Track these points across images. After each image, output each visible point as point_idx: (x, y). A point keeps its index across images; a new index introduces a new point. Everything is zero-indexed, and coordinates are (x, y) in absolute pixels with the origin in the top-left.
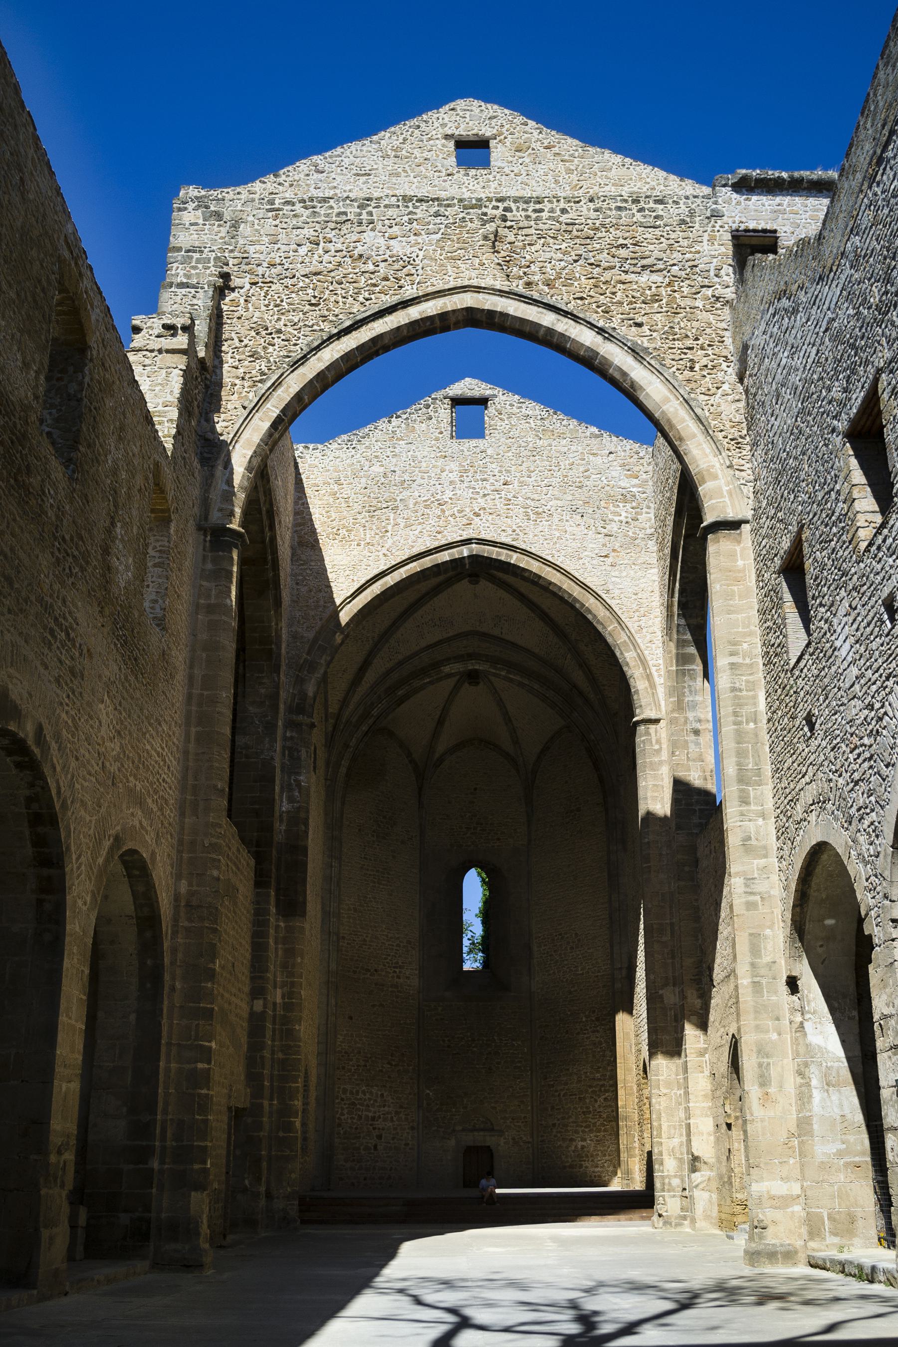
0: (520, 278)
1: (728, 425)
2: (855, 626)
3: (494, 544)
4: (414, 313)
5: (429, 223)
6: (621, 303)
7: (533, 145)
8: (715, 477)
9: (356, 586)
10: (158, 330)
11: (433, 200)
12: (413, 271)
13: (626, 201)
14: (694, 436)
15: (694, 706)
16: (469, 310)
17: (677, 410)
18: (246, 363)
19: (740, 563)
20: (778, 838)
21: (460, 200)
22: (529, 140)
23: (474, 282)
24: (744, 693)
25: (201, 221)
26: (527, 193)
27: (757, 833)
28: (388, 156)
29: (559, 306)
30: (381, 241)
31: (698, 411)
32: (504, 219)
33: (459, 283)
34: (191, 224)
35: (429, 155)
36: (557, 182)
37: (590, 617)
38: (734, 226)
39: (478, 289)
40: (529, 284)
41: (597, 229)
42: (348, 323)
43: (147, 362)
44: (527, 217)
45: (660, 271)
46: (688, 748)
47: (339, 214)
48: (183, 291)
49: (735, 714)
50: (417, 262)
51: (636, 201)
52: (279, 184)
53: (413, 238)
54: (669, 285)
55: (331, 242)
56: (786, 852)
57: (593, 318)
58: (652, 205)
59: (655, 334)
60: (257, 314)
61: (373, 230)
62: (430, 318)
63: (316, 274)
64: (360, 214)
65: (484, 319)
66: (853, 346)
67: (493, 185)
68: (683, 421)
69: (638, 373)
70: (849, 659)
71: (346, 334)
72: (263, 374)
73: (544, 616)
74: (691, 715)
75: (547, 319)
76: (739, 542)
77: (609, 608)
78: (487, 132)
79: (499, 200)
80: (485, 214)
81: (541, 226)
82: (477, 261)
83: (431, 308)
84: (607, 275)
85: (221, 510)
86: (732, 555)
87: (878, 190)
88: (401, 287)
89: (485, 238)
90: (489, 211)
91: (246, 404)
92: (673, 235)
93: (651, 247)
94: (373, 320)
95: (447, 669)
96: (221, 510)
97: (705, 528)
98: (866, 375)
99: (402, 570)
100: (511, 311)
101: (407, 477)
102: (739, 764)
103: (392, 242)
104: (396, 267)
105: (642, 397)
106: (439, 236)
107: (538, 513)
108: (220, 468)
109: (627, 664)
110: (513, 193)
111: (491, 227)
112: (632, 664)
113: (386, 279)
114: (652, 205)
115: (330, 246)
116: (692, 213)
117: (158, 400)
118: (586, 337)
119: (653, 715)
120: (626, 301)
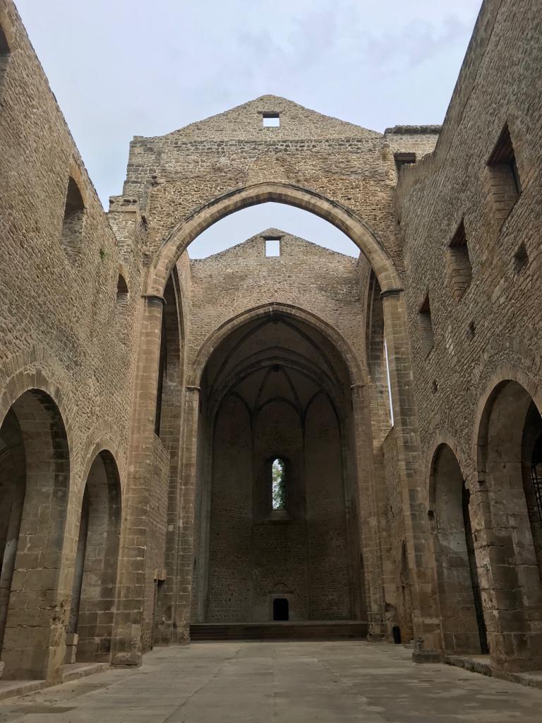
1: (393, 245)
2: (455, 338)
3: (284, 305)
4: (244, 195)
5: (250, 153)
6: (341, 189)
7: (300, 116)
8: (387, 270)
9: (220, 325)
11: (253, 142)
13: (344, 141)
14: (377, 251)
15: (379, 379)
16: (270, 193)
17: (368, 239)
18: (165, 219)
19: (400, 310)
20: (422, 442)
21: (266, 142)
22: (297, 113)
23: (272, 180)
24: (403, 372)
25: (143, 152)
26: (297, 138)
27: (411, 439)
28: (231, 122)
30: (229, 161)
31: (379, 239)
32: (286, 150)
33: (265, 181)
34: (139, 154)
35: (250, 121)
36: (311, 133)
37: (329, 338)
38: (395, 151)
39: (274, 184)
40: (298, 181)
41: (330, 154)
42: (213, 200)
43: (116, 217)
44: (297, 150)
45: (359, 173)
46: (377, 400)
47: (208, 149)
48: (134, 185)
49: (399, 382)
51: (348, 141)
52: (181, 135)
54: (364, 180)
56: (426, 449)
57: (329, 196)
58: (355, 143)
59: (357, 204)
60: (169, 196)
61: (224, 156)
62: (252, 198)
63: (198, 177)
64: (218, 149)
66: (452, 204)
67: (281, 135)
68: (371, 244)
69: (349, 222)
70: (453, 353)
71: (212, 205)
72: (172, 224)
73: (309, 339)
74: (378, 384)
76: (398, 300)
77: (339, 334)
78: (277, 110)
79: (283, 142)
80: (277, 148)
81: (304, 154)
82: (273, 171)
83: (251, 193)
84: (336, 176)
85: (153, 288)
86: (395, 307)
87: (463, 127)
88: (237, 183)
89: (277, 159)
90: (279, 147)
91: (165, 238)
92: (366, 157)
93: (355, 163)
94: (225, 199)
95: (263, 364)
96: (153, 288)
97: (382, 294)
98: (457, 217)
99: (242, 318)
100: (289, 194)
101: (242, 274)
102: (401, 406)
103: (233, 162)
105: (351, 233)
106: (255, 159)
107: (304, 290)
108: (152, 268)
109: (348, 360)
110: (290, 138)
111: (280, 154)
112: (350, 360)
113: (230, 179)
114: (355, 143)
115: (204, 164)
116: (375, 146)
117: (121, 235)
118: (326, 206)
119: (360, 384)
120: (344, 188)
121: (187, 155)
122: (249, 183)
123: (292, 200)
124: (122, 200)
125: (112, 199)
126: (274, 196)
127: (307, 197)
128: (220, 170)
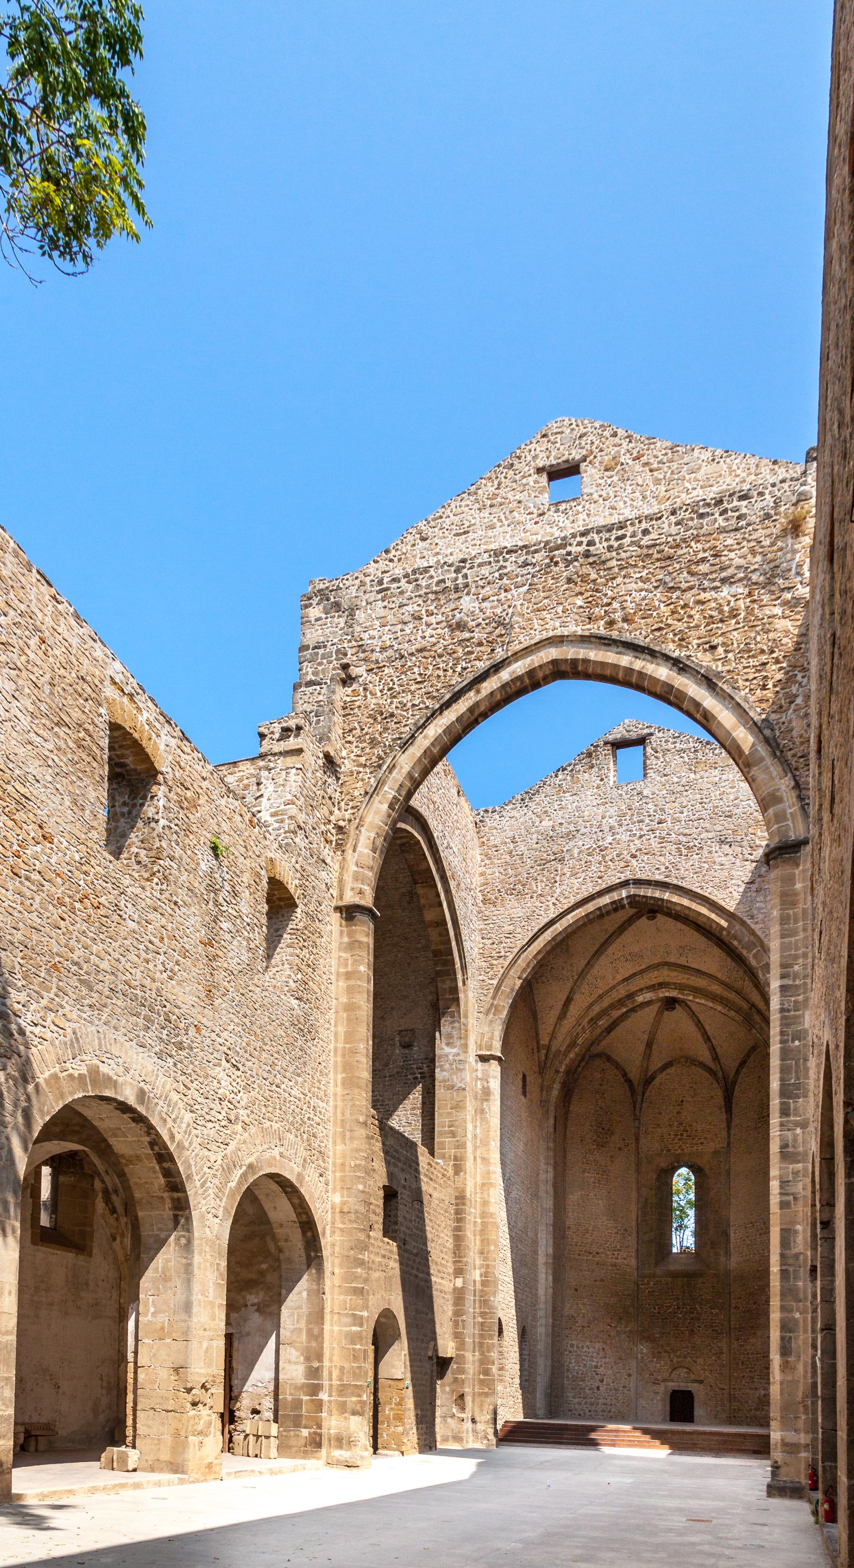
0: (602, 618)
10: (277, 736)
12: (503, 632)
16: (554, 662)
23: (558, 632)
25: (324, 616)
29: (636, 642)
30: (476, 604)
33: (545, 635)
50: (507, 621)
53: (503, 595)
55: (432, 614)
61: (468, 594)
65: (569, 669)
75: (625, 660)
82: (560, 609)
104: (489, 629)
115: (432, 620)
117: (279, 801)
121: (401, 606)
122: (516, 647)
123: (599, 671)
124: (277, 728)
125: (262, 730)
126: (563, 668)
127: (625, 660)
128: (461, 626)
